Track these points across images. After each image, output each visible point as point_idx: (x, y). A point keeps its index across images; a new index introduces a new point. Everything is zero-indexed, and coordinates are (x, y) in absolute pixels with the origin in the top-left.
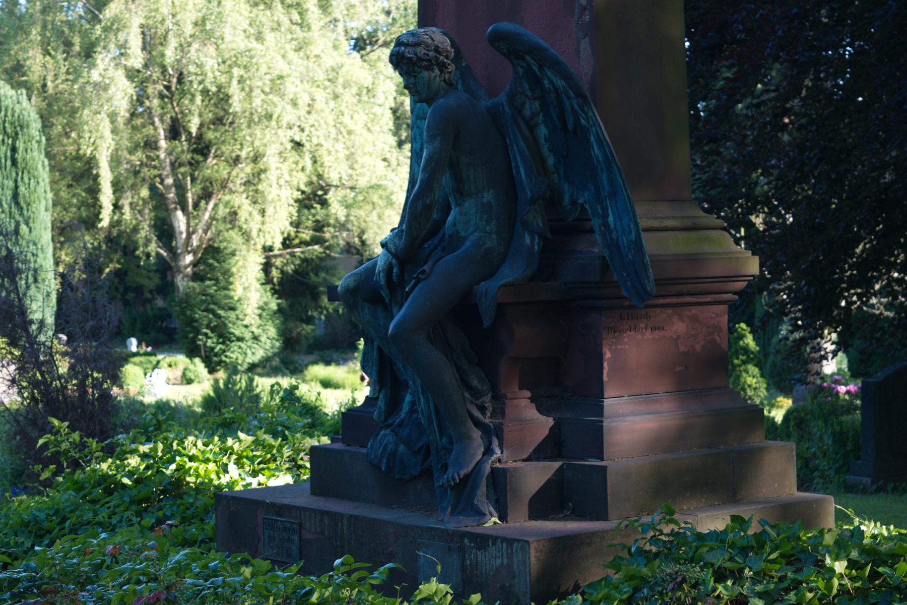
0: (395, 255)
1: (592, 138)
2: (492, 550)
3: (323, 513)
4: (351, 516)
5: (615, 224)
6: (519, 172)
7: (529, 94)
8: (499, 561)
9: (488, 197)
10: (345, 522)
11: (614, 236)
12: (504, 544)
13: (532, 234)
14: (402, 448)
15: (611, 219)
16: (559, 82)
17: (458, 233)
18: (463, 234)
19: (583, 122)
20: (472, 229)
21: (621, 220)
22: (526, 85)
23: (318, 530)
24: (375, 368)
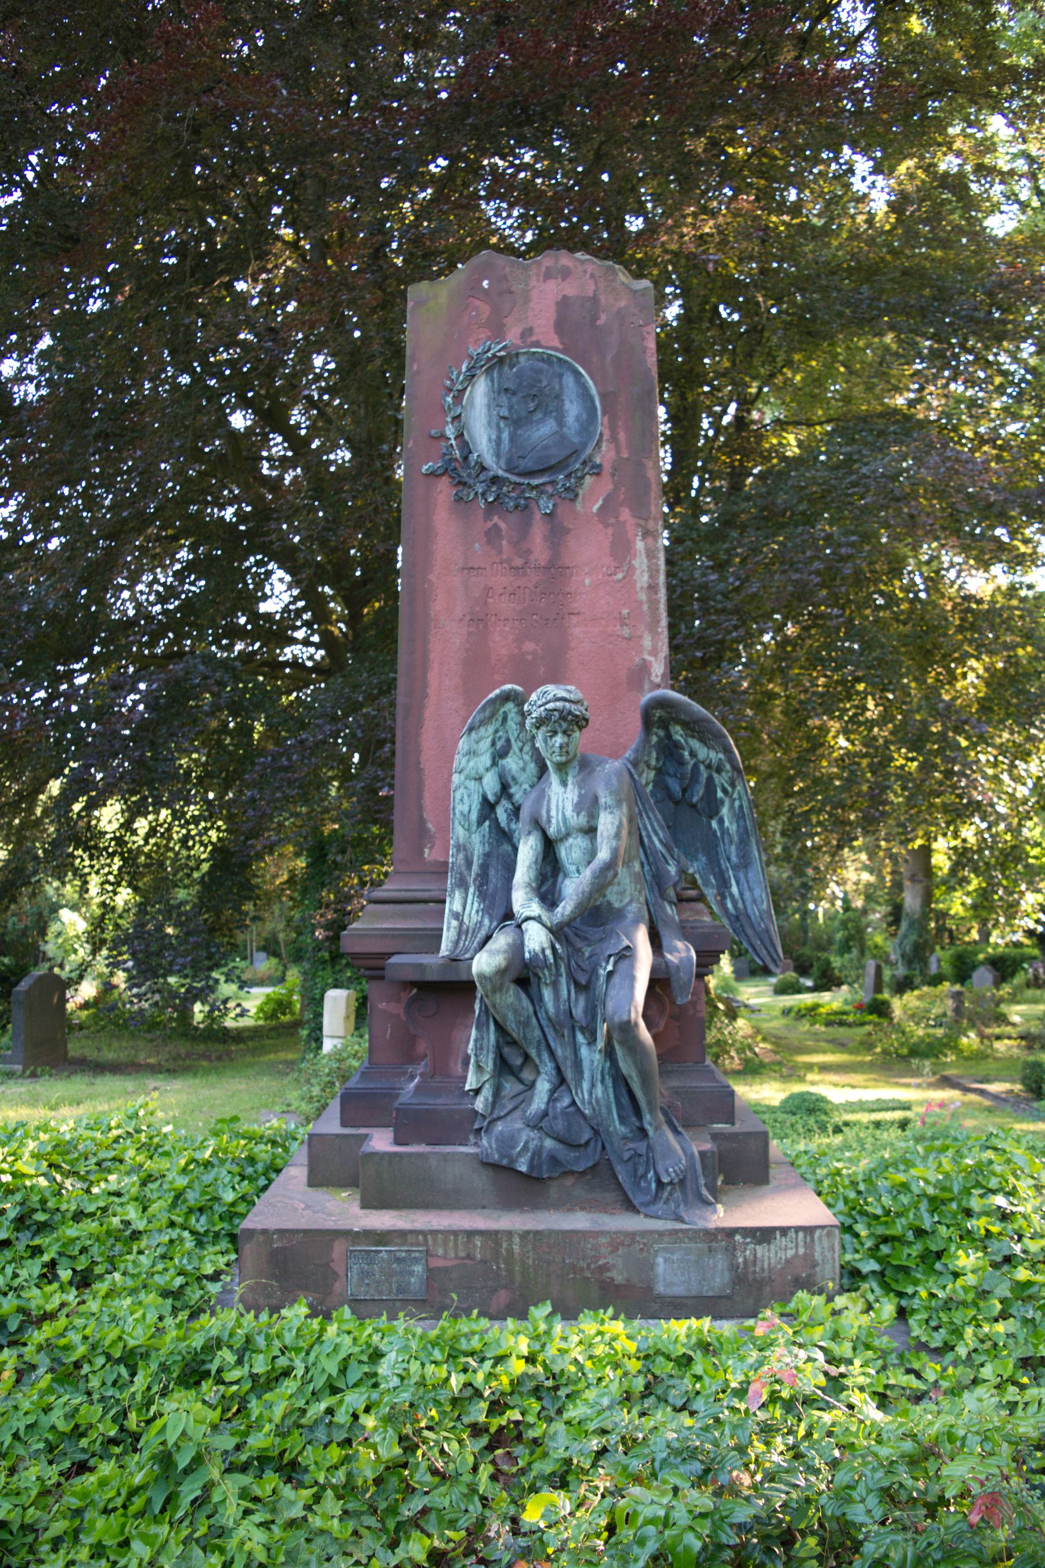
0: (550, 930)
1: (725, 811)
2: (780, 1241)
3: (471, 1234)
4: (527, 1232)
5: (741, 894)
6: (651, 841)
7: (653, 763)
8: (790, 1253)
9: (637, 867)
10: (517, 1240)
11: (740, 905)
12: (801, 1234)
13: (671, 903)
14: (549, 1143)
15: (734, 889)
16: (712, 755)
17: (609, 903)
18: (617, 905)
19: (720, 794)
20: (627, 900)
21: (751, 890)
22: (654, 755)
23: (462, 1254)
24: (491, 1056)
